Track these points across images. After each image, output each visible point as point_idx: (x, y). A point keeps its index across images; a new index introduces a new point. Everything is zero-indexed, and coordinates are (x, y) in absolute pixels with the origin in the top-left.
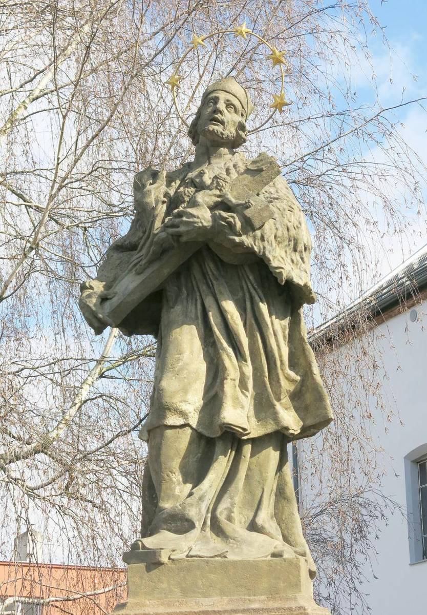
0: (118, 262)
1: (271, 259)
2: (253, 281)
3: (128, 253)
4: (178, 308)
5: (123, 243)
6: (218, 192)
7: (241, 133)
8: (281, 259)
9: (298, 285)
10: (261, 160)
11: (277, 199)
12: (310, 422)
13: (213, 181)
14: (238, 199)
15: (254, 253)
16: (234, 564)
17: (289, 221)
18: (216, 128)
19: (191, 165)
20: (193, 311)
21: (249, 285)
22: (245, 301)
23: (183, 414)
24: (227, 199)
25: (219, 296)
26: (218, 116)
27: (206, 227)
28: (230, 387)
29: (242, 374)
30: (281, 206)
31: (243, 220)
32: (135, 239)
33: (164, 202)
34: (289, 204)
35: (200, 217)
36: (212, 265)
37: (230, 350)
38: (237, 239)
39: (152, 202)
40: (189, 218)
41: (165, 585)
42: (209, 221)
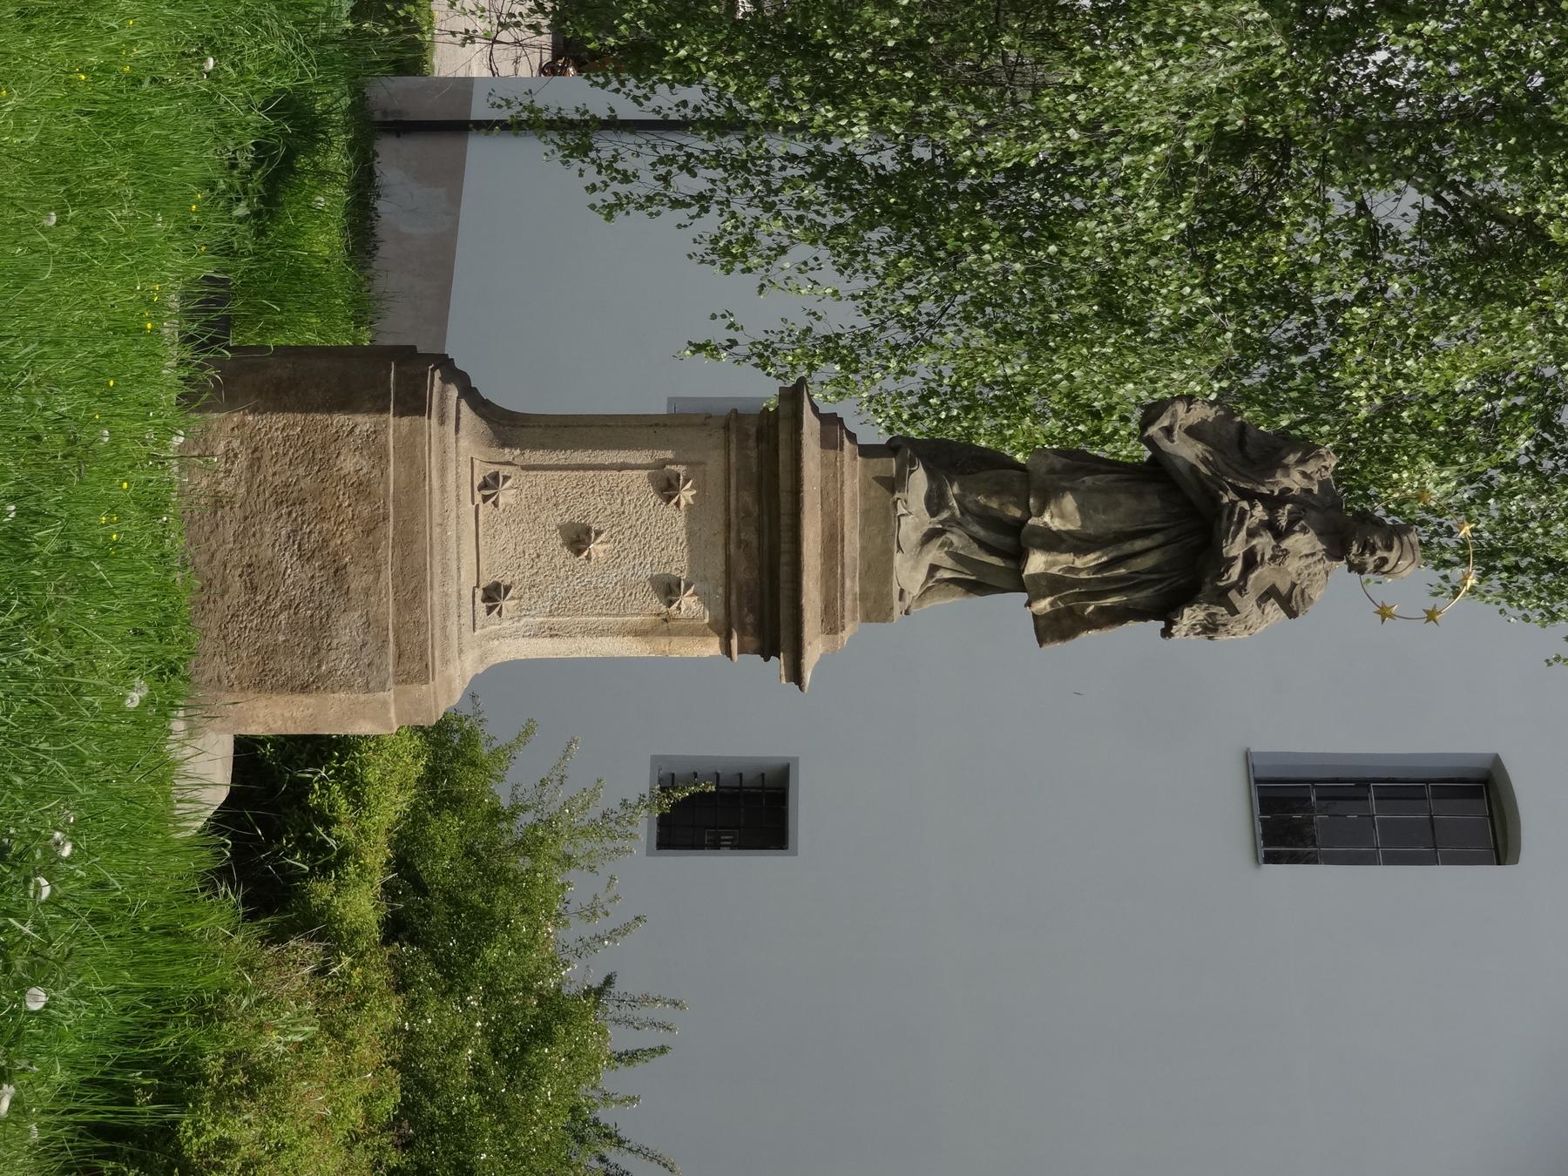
4: (1157, 504)
6: (1267, 557)
16: (891, 560)
23: (1040, 514)
28: (1066, 559)
29: (1081, 570)
37: (1104, 559)
38: (1208, 580)
41: (872, 494)
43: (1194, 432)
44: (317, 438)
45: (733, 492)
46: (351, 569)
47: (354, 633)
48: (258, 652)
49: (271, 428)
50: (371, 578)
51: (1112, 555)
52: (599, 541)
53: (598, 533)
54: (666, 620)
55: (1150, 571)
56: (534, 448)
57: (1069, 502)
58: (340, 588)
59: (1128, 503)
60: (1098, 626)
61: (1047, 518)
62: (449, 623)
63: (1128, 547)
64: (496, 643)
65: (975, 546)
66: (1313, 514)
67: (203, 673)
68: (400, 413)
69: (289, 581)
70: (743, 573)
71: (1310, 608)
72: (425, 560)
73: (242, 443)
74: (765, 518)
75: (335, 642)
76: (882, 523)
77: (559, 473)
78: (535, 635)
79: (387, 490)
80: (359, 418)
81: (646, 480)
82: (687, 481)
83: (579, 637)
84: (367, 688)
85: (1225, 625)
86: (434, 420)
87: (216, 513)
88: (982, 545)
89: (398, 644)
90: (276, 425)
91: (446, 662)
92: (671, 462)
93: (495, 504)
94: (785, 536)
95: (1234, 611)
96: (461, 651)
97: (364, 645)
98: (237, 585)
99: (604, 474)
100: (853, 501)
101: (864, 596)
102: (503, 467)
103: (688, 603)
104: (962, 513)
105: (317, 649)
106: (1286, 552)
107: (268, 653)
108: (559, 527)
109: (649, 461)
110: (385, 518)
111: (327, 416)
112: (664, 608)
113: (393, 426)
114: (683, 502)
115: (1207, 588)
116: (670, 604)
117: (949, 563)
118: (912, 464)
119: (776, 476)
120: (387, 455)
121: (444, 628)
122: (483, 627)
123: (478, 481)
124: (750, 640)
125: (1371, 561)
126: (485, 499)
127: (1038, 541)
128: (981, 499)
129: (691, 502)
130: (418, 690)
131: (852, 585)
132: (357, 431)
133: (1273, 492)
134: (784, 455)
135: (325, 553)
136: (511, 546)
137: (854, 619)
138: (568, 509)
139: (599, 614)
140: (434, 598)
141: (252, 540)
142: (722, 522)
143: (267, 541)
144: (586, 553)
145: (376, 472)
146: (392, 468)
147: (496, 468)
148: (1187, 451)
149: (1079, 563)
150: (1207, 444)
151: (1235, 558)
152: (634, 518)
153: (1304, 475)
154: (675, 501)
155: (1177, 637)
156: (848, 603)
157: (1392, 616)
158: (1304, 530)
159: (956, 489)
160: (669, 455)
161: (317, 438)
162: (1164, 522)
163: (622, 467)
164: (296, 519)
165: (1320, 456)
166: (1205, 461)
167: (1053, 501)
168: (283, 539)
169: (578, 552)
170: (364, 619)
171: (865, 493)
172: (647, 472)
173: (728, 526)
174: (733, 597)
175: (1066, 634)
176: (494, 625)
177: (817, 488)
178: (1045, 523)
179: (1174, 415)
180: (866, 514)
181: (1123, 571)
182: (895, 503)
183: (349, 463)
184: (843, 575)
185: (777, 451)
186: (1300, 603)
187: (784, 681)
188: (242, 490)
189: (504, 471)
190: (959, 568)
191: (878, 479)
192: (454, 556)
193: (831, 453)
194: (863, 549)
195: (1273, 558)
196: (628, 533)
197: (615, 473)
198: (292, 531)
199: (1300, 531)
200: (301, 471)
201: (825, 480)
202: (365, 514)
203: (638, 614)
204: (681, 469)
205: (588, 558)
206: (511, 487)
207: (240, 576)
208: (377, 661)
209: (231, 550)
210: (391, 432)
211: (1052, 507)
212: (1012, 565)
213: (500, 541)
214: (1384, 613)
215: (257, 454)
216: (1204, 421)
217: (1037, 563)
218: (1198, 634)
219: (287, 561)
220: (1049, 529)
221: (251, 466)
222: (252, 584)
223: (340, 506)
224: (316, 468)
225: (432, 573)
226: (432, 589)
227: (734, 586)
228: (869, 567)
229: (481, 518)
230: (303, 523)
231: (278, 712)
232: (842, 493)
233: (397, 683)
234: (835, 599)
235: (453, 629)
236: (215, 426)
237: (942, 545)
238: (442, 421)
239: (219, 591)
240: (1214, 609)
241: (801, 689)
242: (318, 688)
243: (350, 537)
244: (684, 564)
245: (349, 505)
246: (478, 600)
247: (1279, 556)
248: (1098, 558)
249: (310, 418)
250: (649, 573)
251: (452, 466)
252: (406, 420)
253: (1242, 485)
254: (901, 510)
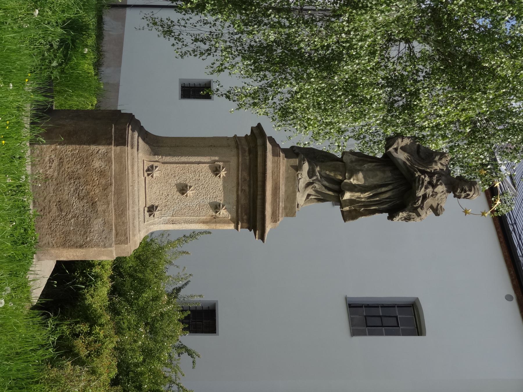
4: (390, 175)
6: (430, 195)
12: (345, 214)
16: (296, 195)
18: (459, 190)
23: (350, 178)
25: (392, 191)
28: (358, 194)
29: (362, 198)
37: (371, 194)
38: (410, 204)
41: (290, 171)
43: (403, 149)
44: (84, 154)
45: (240, 172)
46: (98, 203)
47: (99, 227)
48: (63, 233)
49: (66, 150)
50: (106, 206)
51: (374, 193)
52: (190, 190)
53: (190, 187)
54: (215, 218)
55: (387, 198)
56: (166, 155)
57: (361, 175)
58: (94, 210)
59: (380, 175)
60: (365, 215)
61: (352, 180)
62: (135, 222)
63: (380, 190)
64: (152, 226)
65: (324, 188)
66: (443, 178)
67: (42, 241)
68: (116, 145)
69: (75, 207)
70: (243, 201)
71: (444, 213)
72: (126, 199)
73: (55, 156)
74: (252, 182)
75: (92, 229)
76: (293, 181)
77: (176, 165)
78: (167, 223)
79: (111, 174)
80: (101, 147)
81: (208, 168)
82: (223, 168)
83: (183, 224)
84: (105, 246)
85: (413, 218)
86: (129, 147)
87: (46, 182)
88: (326, 187)
89: (116, 230)
90: (69, 149)
91: (134, 235)
92: (217, 161)
93: (152, 177)
94: (259, 189)
95: (419, 215)
96: (139, 231)
97: (103, 231)
98: (54, 209)
99: (192, 165)
100: (283, 175)
101: (285, 208)
102: (155, 163)
103: (223, 213)
104: (321, 178)
105: (86, 232)
106: (437, 193)
107: (67, 234)
108: (176, 185)
109: (209, 160)
110: (111, 184)
111: (88, 146)
112: (214, 214)
113: (114, 150)
114: (222, 176)
115: (409, 207)
116: (216, 212)
117: (313, 193)
118: (304, 161)
119: (256, 166)
120: (112, 161)
121: (133, 223)
122: (148, 221)
123: (146, 168)
124: (245, 225)
125: (463, 195)
126: (148, 175)
127: (347, 187)
128: (328, 172)
129: (225, 176)
130: (124, 246)
131: (282, 205)
132: (100, 152)
133: (431, 171)
134: (260, 160)
135: (88, 197)
136: (158, 191)
137: (282, 216)
138: (179, 178)
139: (190, 216)
140: (130, 213)
141: (60, 192)
142: (236, 182)
143: (66, 192)
144: (186, 194)
145: (107, 167)
146: (113, 166)
147: (152, 163)
148: (402, 156)
149: (362, 196)
150: (408, 153)
151: (420, 197)
152: (203, 181)
153: (441, 164)
154: (219, 175)
155: (395, 221)
156: (280, 211)
157: (469, 213)
158: (441, 184)
159: (318, 169)
160: (217, 158)
161: (84, 154)
162: (392, 181)
163: (199, 163)
164: (77, 184)
165: (446, 157)
166: (408, 159)
167: (355, 175)
168: (72, 192)
169: (183, 194)
170: (103, 221)
171: (287, 171)
172: (208, 165)
173: (238, 184)
174: (240, 210)
175: (354, 218)
176: (152, 220)
177: (271, 171)
178: (351, 182)
179: (398, 144)
180: (287, 179)
181: (378, 199)
182: (298, 175)
183: (97, 164)
184: (279, 201)
185: (257, 158)
186: (440, 211)
187: (257, 239)
188: (56, 174)
189: (156, 164)
190: (317, 195)
191: (292, 166)
192: (137, 197)
193: (276, 158)
194: (286, 191)
195: (432, 196)
196: (201, 187)
197: (196, 165)
198: (75, 189)
199: (440, 185)
200: (79, 167)
201: (273, 168)
202: (103, 183)
203: (205, 216)
204: (221, 164)
205: (187, 196)
206: (158, 170)
207: (56, 205)
208: (108, 237)
209: (52, 196)
210: (113, 152)
211: (354, 177)
212: (336, 194)
213: (154, 190)
214: (466, 212)
215: (61, 160)
216: (407, 144)
217: (347, 196)
218: (403, 220)
219: (74, 200)
220: (352, 184)
221: (59, 165)
222: (60, 208)
223: (94, 180)
224: (84, 166)
225: (129, 204)
226: (129, 210)
227: (240, 206)
228: (288, 197)
229: (147, 182)
230: (80, 186)
231: (71, 254)
232: (279, 172)
233: (116, 244)
234: (276, 210)
235: (136, 223)
236: (45, 150)
237: (312, 187)
238: (132, 148)
239: (48, 211)
240: (411, 214)
241: (263, 242)
242: (86, 246)
243: (97, 191)
244: (222, 198)
245: (97, 179)
246: (146, 212)
247: (434, 194)
248: (369, 194)
249: (82, 147)
250: (209, 201)
251: (136, 164)
252: (118, 148)
253: (420, 168)
254: (300, 177)
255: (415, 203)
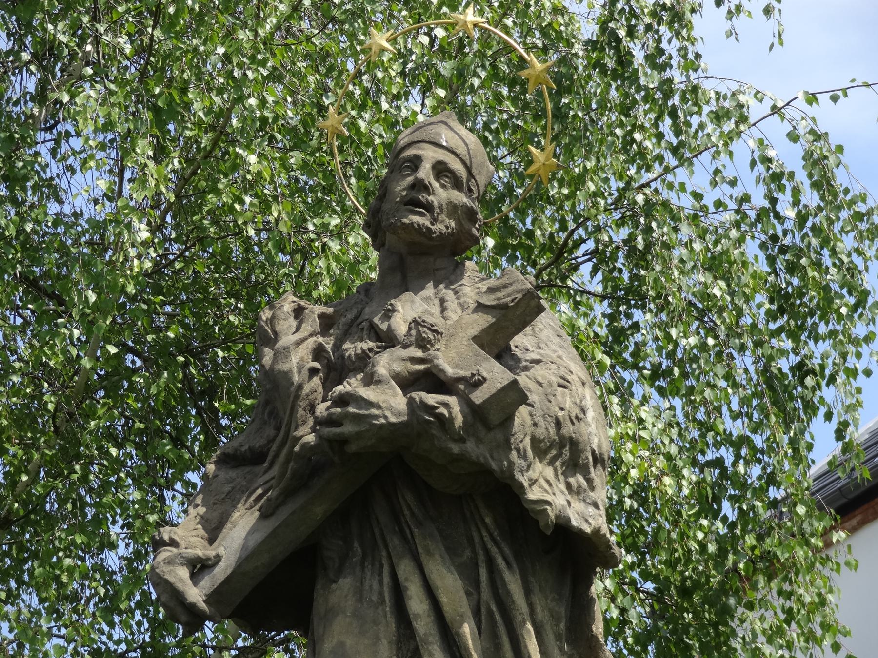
0: (227, 488)
1: (526, 484)
2: (492, 527)
3: (247, 469)
4: (346, 583)
5: (236, 450)
6: (419, 354)
7: (466, 224)
8: (546, 486)
9: (580, 533)
10: (505, 286)
11: (538, 362)
13: (410, 329)
14: (457, 366)
15: (489, 472)
17: (562, 409)
18: (416, 219)
19: (372, 290)
20: (376, 586)
21: (485, 534)
22: (476, 566)
24: (436, 366)
25: (424, 558)
26: (423, 197)
27: (393, 424)
30: (544, 377)
31: (467, 410)
32: (258, 442)
33: (313, 372)
34: (562, 373)
35: (383, 405)
36: (410, 498)
38: (455, 448)
39: (290, 371)
40: (360, 408)
42: (400, 414)
85: (558, 424)
151: (411, 402)
181: (467, 630)
186: (510, 290)
195: (423, 344)
255: (444, 422)
